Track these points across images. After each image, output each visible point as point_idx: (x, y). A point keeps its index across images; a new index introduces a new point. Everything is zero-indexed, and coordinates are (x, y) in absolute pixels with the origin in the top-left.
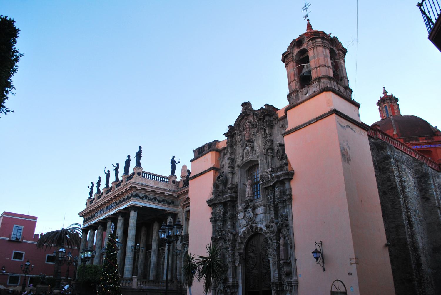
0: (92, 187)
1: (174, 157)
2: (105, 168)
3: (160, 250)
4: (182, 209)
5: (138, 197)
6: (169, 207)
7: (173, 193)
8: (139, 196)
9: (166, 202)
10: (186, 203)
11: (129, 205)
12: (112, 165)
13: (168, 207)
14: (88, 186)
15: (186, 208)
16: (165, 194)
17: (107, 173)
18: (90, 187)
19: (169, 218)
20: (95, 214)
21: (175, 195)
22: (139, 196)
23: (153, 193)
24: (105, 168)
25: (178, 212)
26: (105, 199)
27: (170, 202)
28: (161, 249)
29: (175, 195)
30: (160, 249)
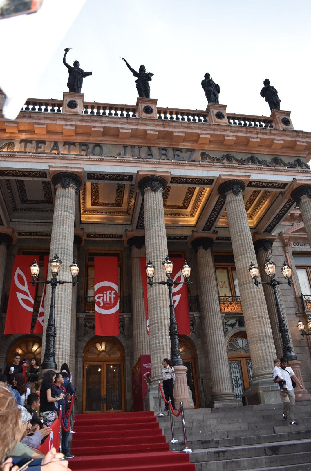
2: (67, 50)
12: (125, 60)
15: (293, 246)
17: (73, 66)
24: (67, 50)
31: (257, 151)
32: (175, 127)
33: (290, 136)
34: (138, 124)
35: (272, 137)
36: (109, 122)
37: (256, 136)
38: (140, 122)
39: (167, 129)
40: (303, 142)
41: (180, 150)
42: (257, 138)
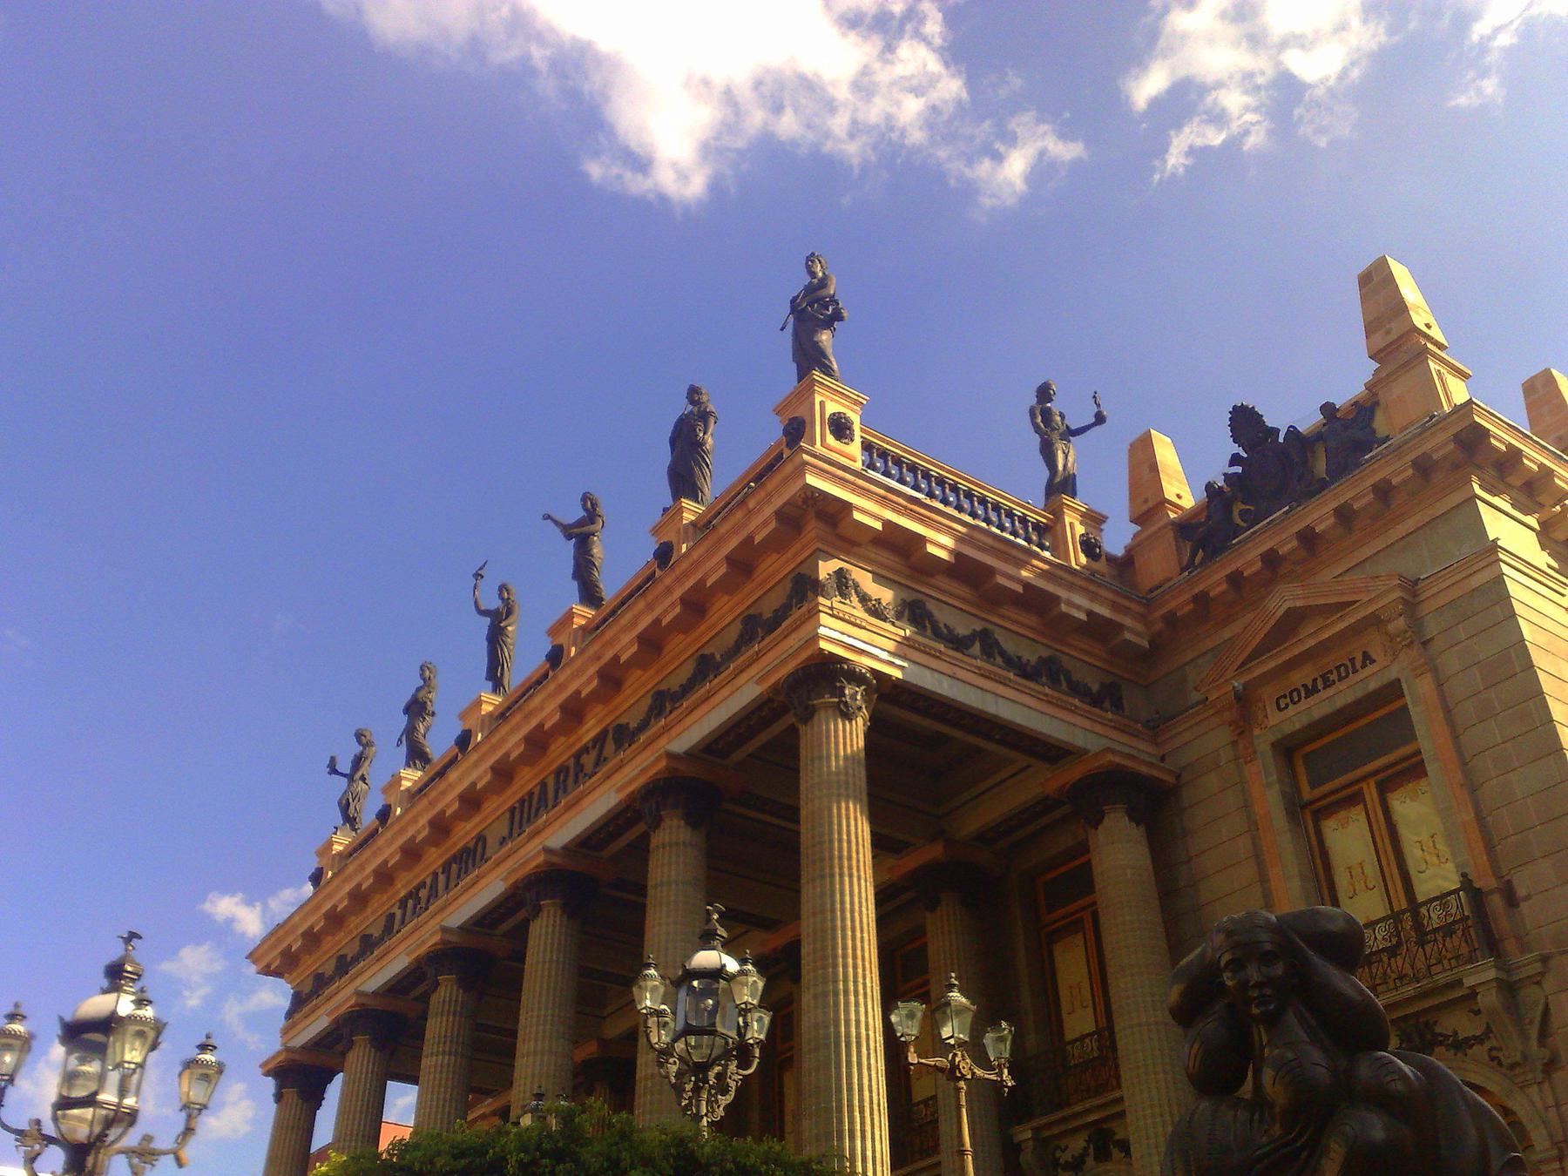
0: (358, 761)
1: (1044, 393)
3: (1017, 1149)
4: (1223, 736)
5: (854, 598)
6: (1098, 728)
7: (1115, 607)
8: (864, 599)
9: (1064, 684)
10: (1280, 660)
11: (784, 662)
12: (547, 517)
13: (1087, 723)
14: (333, 759)
15: (1275, 717)
16: (1064, 608)
17: (494, 603)
18: (345, 766)
19: (1107, 822)
20: (393, 916)
21: (1132, 631)
22: (864, 599)
23: (964, 591)
24: (478, 576)
25: (1178, 777)
26: (503, 740)
27: (1095, 688)
28: (1036, 1130)
29: (1134, 632)
30: (1024, 1134)
31: (709, 629)
32: (541, 708)
33: (734, 531)
34: (494, 749)
35: (699, 575)
36: (460, 779)
37: (669, 601)
38: (494, 740)
39: (534, 722)
40: (765, 523)
41: (585, 750)
42: (673, 605)
